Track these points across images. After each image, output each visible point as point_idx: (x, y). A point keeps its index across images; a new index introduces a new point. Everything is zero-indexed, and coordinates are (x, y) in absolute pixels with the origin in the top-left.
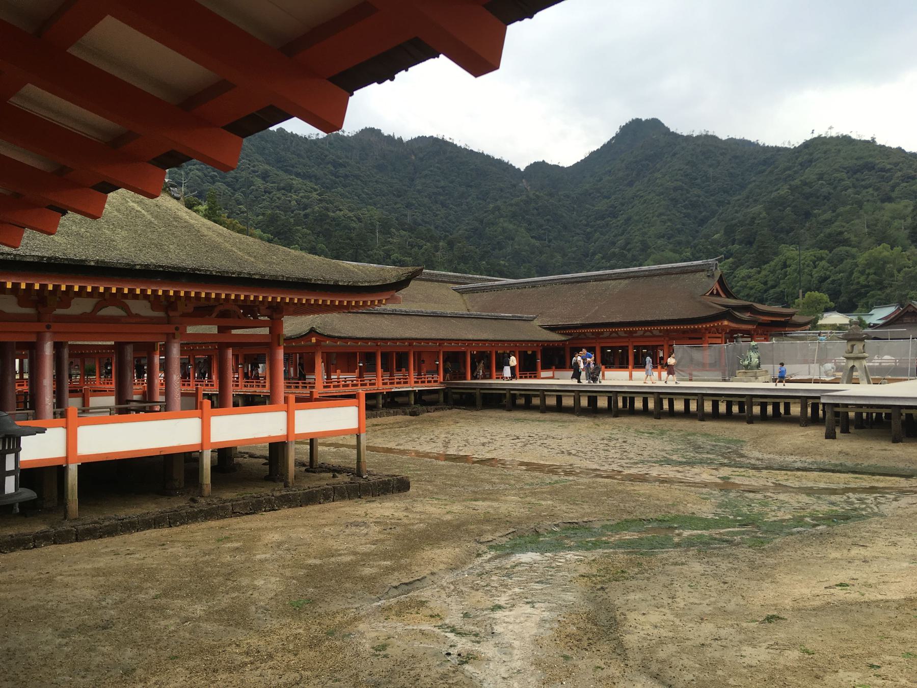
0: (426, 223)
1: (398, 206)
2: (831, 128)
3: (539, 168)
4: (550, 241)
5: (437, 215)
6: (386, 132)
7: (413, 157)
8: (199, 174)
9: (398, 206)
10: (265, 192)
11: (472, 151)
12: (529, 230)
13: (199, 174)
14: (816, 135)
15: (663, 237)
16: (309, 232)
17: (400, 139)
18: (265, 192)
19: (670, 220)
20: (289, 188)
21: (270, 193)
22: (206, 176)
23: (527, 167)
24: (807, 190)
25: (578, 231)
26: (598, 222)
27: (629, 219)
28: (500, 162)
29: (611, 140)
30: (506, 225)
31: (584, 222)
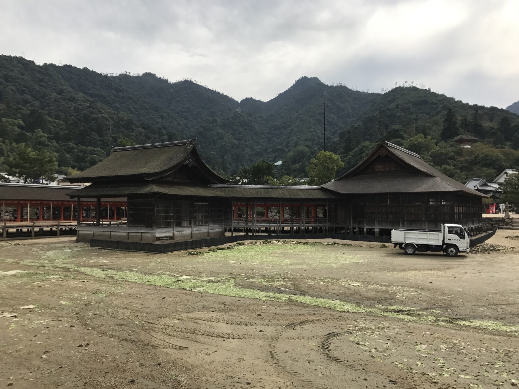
0: (171, 127)
1: (154, 116)
2: (406, 82)
3: (249, 102)
4: (246, 141)
5: (179, 124)
6: (158, 76)
7: (172, 90)
8: (13, 88)
9: (154, 116)
10: (55, 101)
11: (209, 89)
12: (233, 135)
13: (13, 88)
14: (398, 86)
15: (309, 140)
16: (62, 123)
17: (166, 81)
18: (55, 101)
19: (314, 131)
20: (72, 99)
21: (58, 102)
22: (18, 89)
23: (242, 101)
24: (389, 113)
25: (263, 136)
26: (275, 132)
27: (292, 130)
28: (226, 97)
29: (291, 88)
30: (219, 130)
31: (267, 131)
